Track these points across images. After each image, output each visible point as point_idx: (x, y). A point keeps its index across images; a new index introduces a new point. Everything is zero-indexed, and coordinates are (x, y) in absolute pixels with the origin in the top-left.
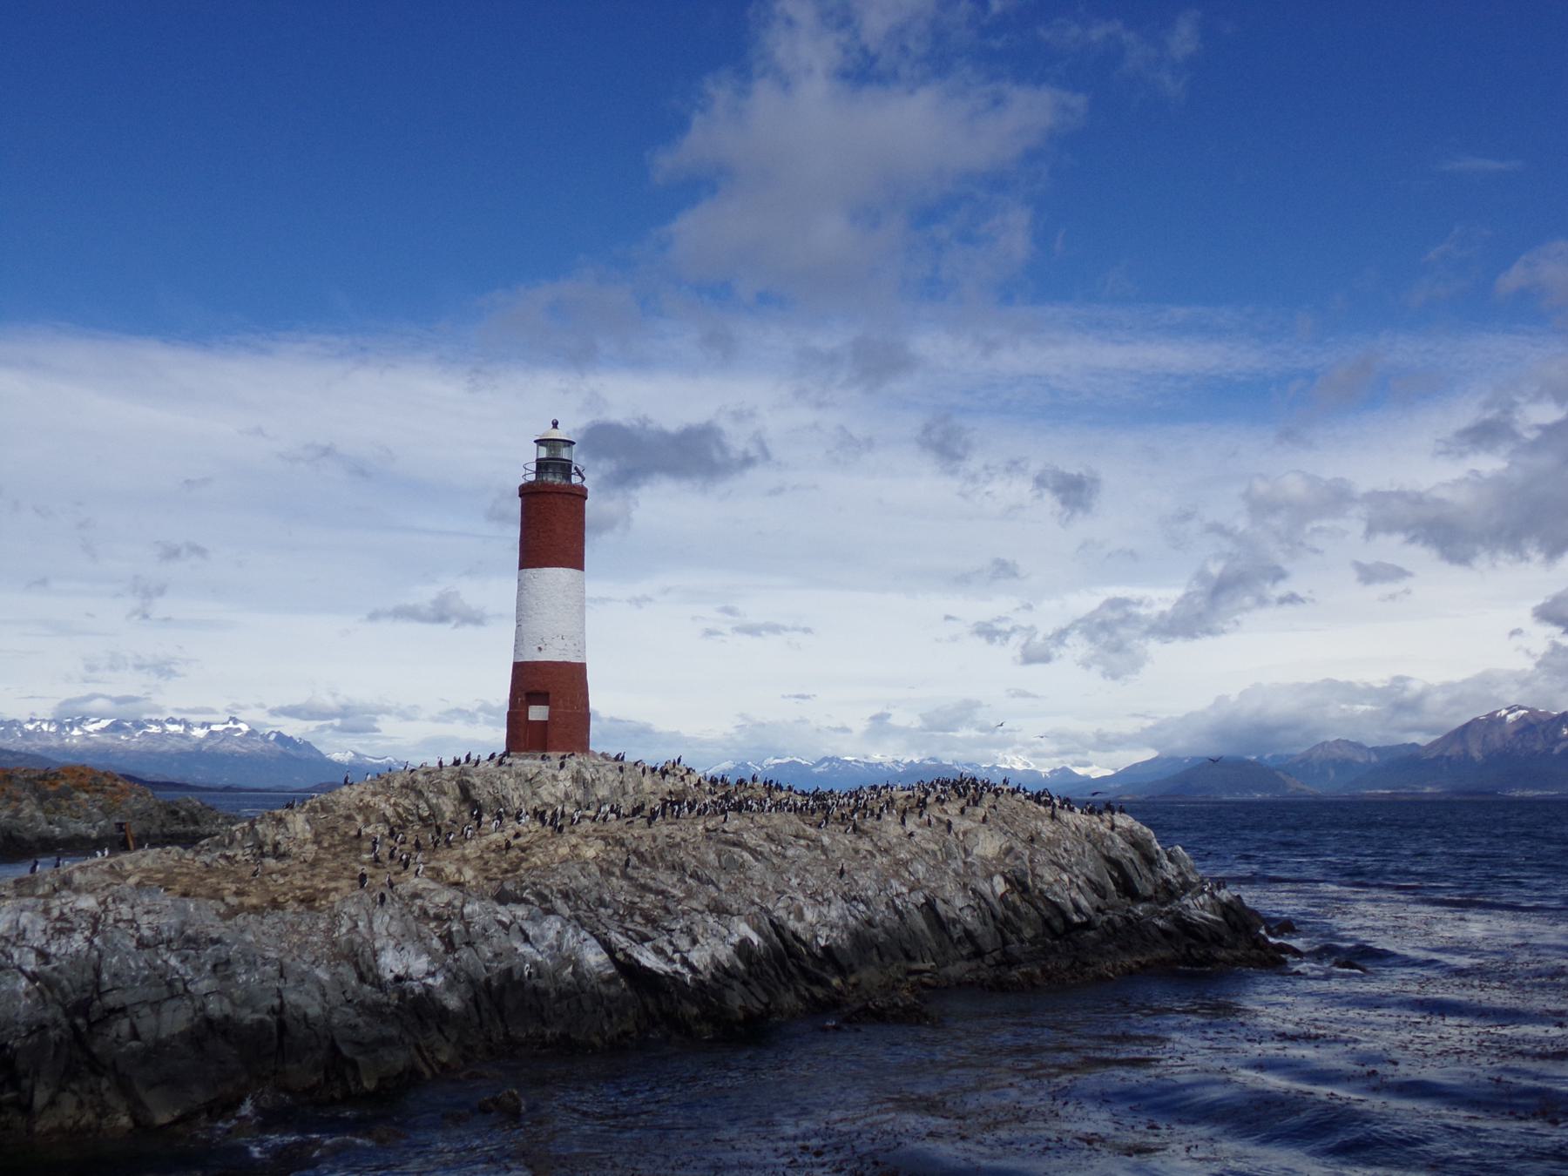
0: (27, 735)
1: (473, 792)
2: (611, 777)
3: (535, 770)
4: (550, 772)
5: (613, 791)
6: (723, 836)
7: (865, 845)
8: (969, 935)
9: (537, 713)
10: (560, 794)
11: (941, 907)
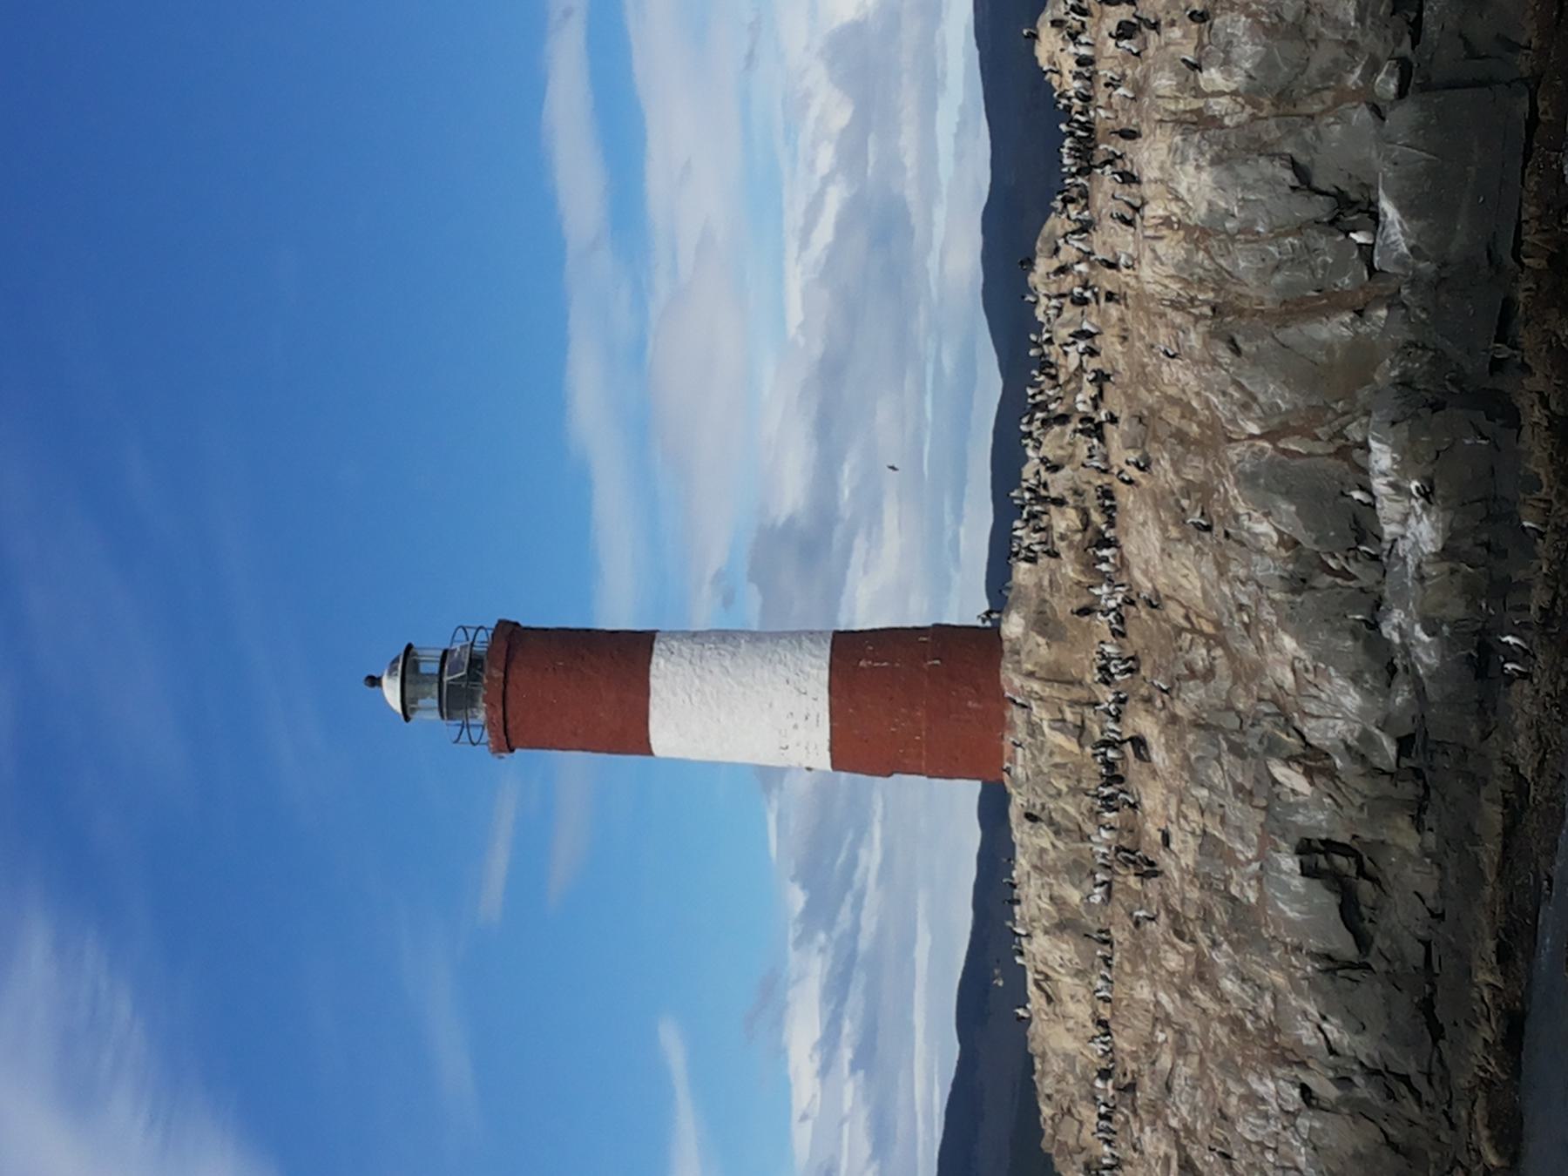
2: (1046, 844)
5: (1078, 869)
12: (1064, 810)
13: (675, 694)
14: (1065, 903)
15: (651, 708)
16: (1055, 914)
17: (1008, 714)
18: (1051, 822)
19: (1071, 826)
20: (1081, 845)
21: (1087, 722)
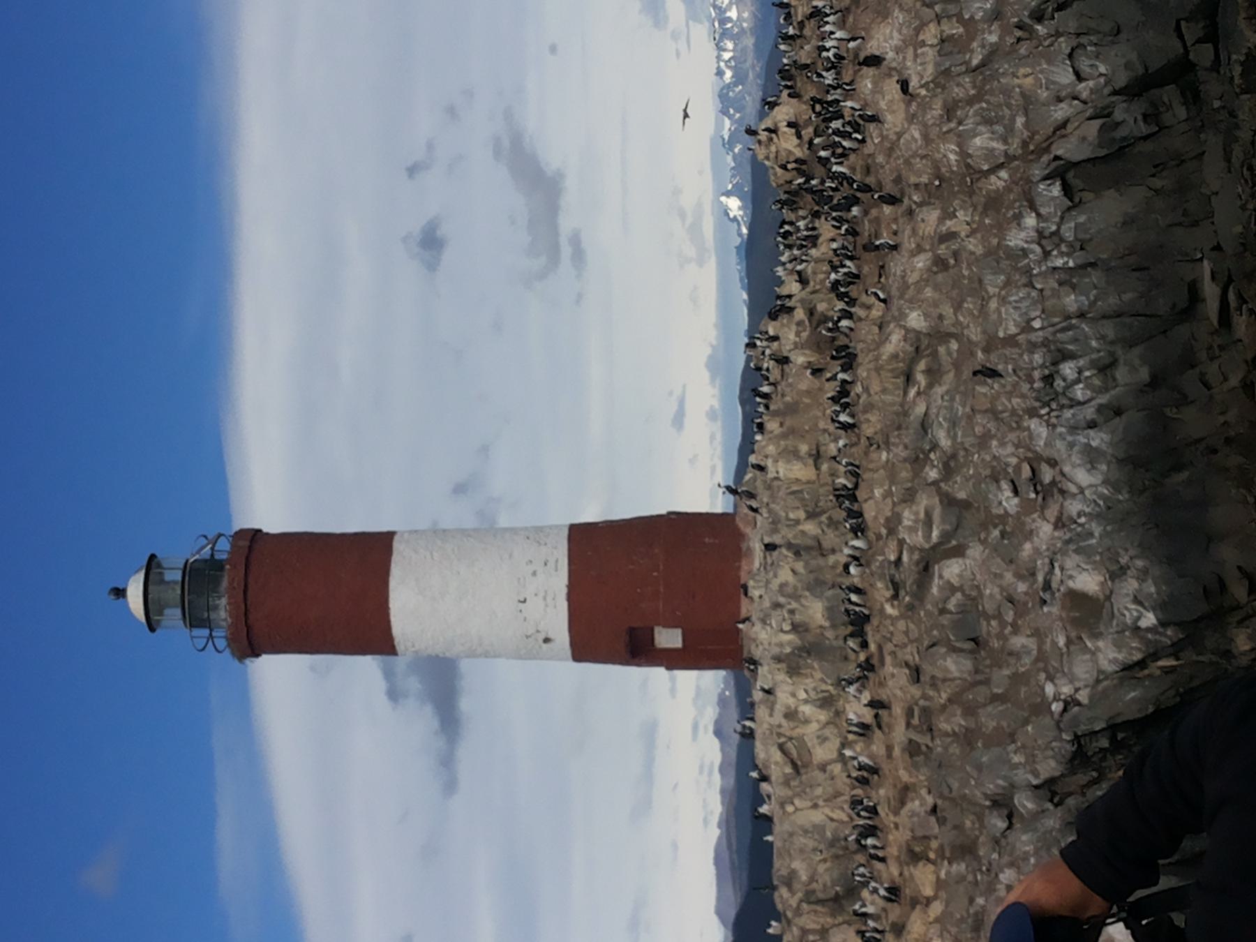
0: (739, 78)
1: (821, 896)
2: (785, 575)
3: (777, 756)
4: (778, 718)
5: (816, 585)
6: (908, 575)
7: (930, 219)
8: (1134, 90)
9: (668, 638)
10: (823, 716)
11: (1067, 149)
12: (803, 532)
13: (416, 552)
14: (807, 630)
15: (393, 565)
16: (799, 642)
17: (744, 546)
18: (789, 546)
19: (810, 542)
20: (821, 561)
21: (822, 449)
